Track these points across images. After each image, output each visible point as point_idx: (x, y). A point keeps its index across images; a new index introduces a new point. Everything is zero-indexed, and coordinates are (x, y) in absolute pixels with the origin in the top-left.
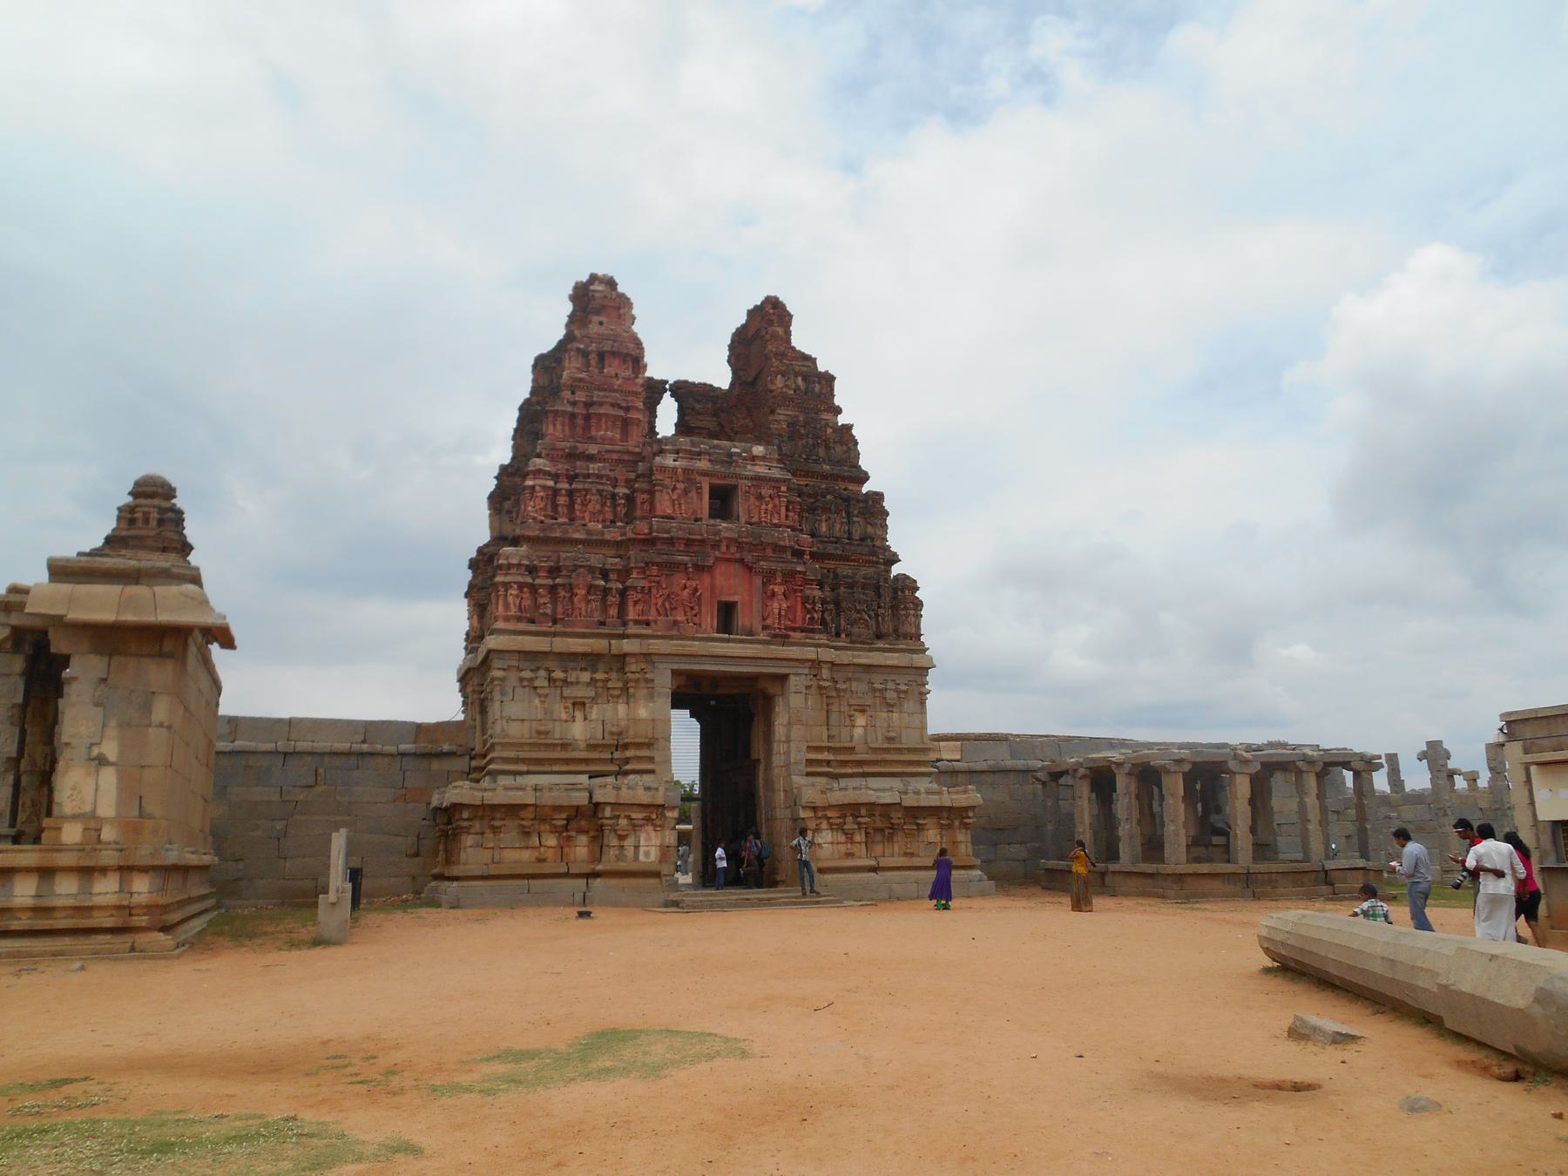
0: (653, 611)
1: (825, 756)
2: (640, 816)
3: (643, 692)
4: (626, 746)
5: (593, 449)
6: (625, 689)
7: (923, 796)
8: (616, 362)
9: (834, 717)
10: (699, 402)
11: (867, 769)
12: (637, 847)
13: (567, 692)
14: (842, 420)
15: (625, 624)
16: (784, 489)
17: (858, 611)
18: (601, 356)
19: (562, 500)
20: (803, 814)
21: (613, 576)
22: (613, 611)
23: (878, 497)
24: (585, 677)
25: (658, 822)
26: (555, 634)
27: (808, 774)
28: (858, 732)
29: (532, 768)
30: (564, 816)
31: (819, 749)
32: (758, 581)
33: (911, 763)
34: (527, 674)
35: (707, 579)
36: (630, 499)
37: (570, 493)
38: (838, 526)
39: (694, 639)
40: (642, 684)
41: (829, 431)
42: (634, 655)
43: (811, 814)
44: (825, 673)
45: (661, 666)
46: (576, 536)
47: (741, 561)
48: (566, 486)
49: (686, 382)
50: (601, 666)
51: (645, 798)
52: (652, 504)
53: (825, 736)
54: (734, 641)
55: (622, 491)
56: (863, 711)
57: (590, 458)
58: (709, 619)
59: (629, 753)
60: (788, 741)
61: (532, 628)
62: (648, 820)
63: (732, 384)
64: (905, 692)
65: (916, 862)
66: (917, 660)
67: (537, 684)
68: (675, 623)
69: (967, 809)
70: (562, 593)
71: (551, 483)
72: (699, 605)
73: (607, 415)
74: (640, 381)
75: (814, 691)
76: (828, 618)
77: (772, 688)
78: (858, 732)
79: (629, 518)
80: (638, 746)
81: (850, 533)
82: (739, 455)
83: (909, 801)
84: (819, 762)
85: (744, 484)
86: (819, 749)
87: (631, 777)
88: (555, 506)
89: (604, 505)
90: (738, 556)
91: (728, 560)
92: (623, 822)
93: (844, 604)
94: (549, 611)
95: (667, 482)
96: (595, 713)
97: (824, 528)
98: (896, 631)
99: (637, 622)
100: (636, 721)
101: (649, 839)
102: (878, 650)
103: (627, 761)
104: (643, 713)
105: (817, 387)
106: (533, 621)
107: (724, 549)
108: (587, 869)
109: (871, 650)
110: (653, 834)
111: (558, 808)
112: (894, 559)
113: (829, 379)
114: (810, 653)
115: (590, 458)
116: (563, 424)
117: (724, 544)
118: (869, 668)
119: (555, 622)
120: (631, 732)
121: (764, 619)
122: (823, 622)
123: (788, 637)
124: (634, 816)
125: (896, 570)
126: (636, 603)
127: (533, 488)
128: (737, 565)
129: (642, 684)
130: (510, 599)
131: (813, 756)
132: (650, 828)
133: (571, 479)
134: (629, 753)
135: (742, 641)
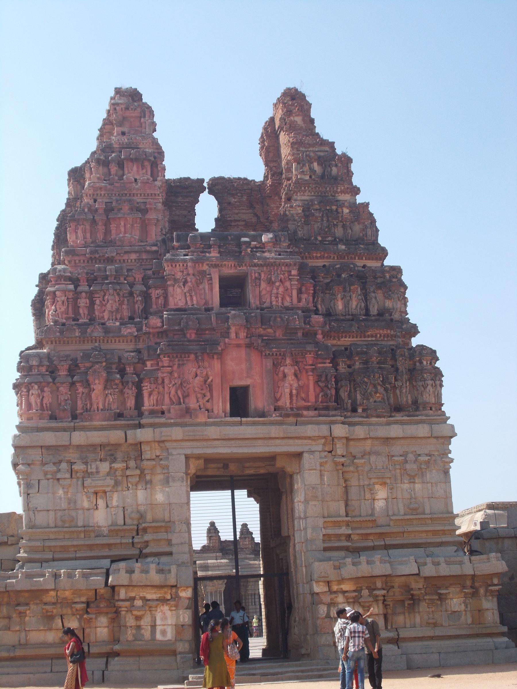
0: (167, 400)
1: (344, 530)
2: (155, 596)
3: (159, 477)
4: (145, 530)
5: (110, 252)
6: (142, 475)
7: (443, 565)
9: (354, 492)
10: (233, 195)
11: (389, 541)
12: (154, 627)
13: (88, 482)
14: (360, 199)
15: (141, 415)
16: (294, 272)
18: (121, 165)
19: (83, 302)
20: (318, 588)
21: (129, 369)
22: (131, 403)
23: (397, 271)
24: (104, 467)
25: (172, 603)
26: (74, 429)
27: (325, 549)
28: (380, 504)
29: (57, 556)
30: (84, 599)
31: (337, 524)
32: (269, 363)
33: (435, 533)
34: (51, 468)
36: (147, 297)
37: (91, 296)
38: (354, 304)
39: (206, 424)
40: (159, 470)
41: (346, 211)
42: (148, 442)
43: (326, 589)
44: (340, 450)
45: (174, 452)
46: (95, 334)
47: (249, 346)
48: (87, 288)
49: (222, 178)
50: (119, 455)
51: (154, 577)
52: (166, 298)
53: (343, 512)
54: (247, 424)
55: (139, 288)
56: (384, 484)
57: (110, 260)
58: (221, 404)
59: (147, 537)
61: (54, 424)
62: (163, 601)
63: (266, 177)
64: (428, 462)
65: (438, 632)
66: (438, 429)
67: (59, 476)
68: (188, 411)
69: (492, 576)
70: (81, 390)
71: (71, 287)
72: (211, 391)
74: (158, 183)
75: (329, 466)
76: (344, 394)
78: (380, 504)
79: (146, 313)
80: (156, 530)
81: (367, 309)
82: (248, 244)
83: (429, 571)
84: (338, 537)
85: (253, 272)
86: (337, 524)
87: (149, 559)
88: (76, 308)
89: (121, 303)
91: (238, 346)
92: (138, 603)
93: (358, 379)
94: (68, 407)
95: (179, 275)
96: (115, 500)
97: (340, 306)
98: (415, 402)
99: (152, 413)
100: (152, 505)
101: (164, 618)
102: (396, 422)
103: (147, 544)
104: (160, 497)
105: (334, 170)
106: (53, 417)
107: (233, 335)
108: (105, 649)
109: (388, 424)
110: (168, 613)
111: (77, 592)
112: (414, 330)
113: (347, 160)
114: (324, 430)
115: (110, 260)
116: (84, 232)
118: (387, 441)
119: (74, 417)
120: (149, 517)
121: (277, 400)
122: (338, 399)
123: (301, 416)
124: (149, 597)
125: (415, 342)
127: (54, 293)
129: (159, 470)
130: (32, 399)
131: (330, 531)
132: (166, 608)
133: (91, 282)
134: (147, 537)
135: (254, 424)
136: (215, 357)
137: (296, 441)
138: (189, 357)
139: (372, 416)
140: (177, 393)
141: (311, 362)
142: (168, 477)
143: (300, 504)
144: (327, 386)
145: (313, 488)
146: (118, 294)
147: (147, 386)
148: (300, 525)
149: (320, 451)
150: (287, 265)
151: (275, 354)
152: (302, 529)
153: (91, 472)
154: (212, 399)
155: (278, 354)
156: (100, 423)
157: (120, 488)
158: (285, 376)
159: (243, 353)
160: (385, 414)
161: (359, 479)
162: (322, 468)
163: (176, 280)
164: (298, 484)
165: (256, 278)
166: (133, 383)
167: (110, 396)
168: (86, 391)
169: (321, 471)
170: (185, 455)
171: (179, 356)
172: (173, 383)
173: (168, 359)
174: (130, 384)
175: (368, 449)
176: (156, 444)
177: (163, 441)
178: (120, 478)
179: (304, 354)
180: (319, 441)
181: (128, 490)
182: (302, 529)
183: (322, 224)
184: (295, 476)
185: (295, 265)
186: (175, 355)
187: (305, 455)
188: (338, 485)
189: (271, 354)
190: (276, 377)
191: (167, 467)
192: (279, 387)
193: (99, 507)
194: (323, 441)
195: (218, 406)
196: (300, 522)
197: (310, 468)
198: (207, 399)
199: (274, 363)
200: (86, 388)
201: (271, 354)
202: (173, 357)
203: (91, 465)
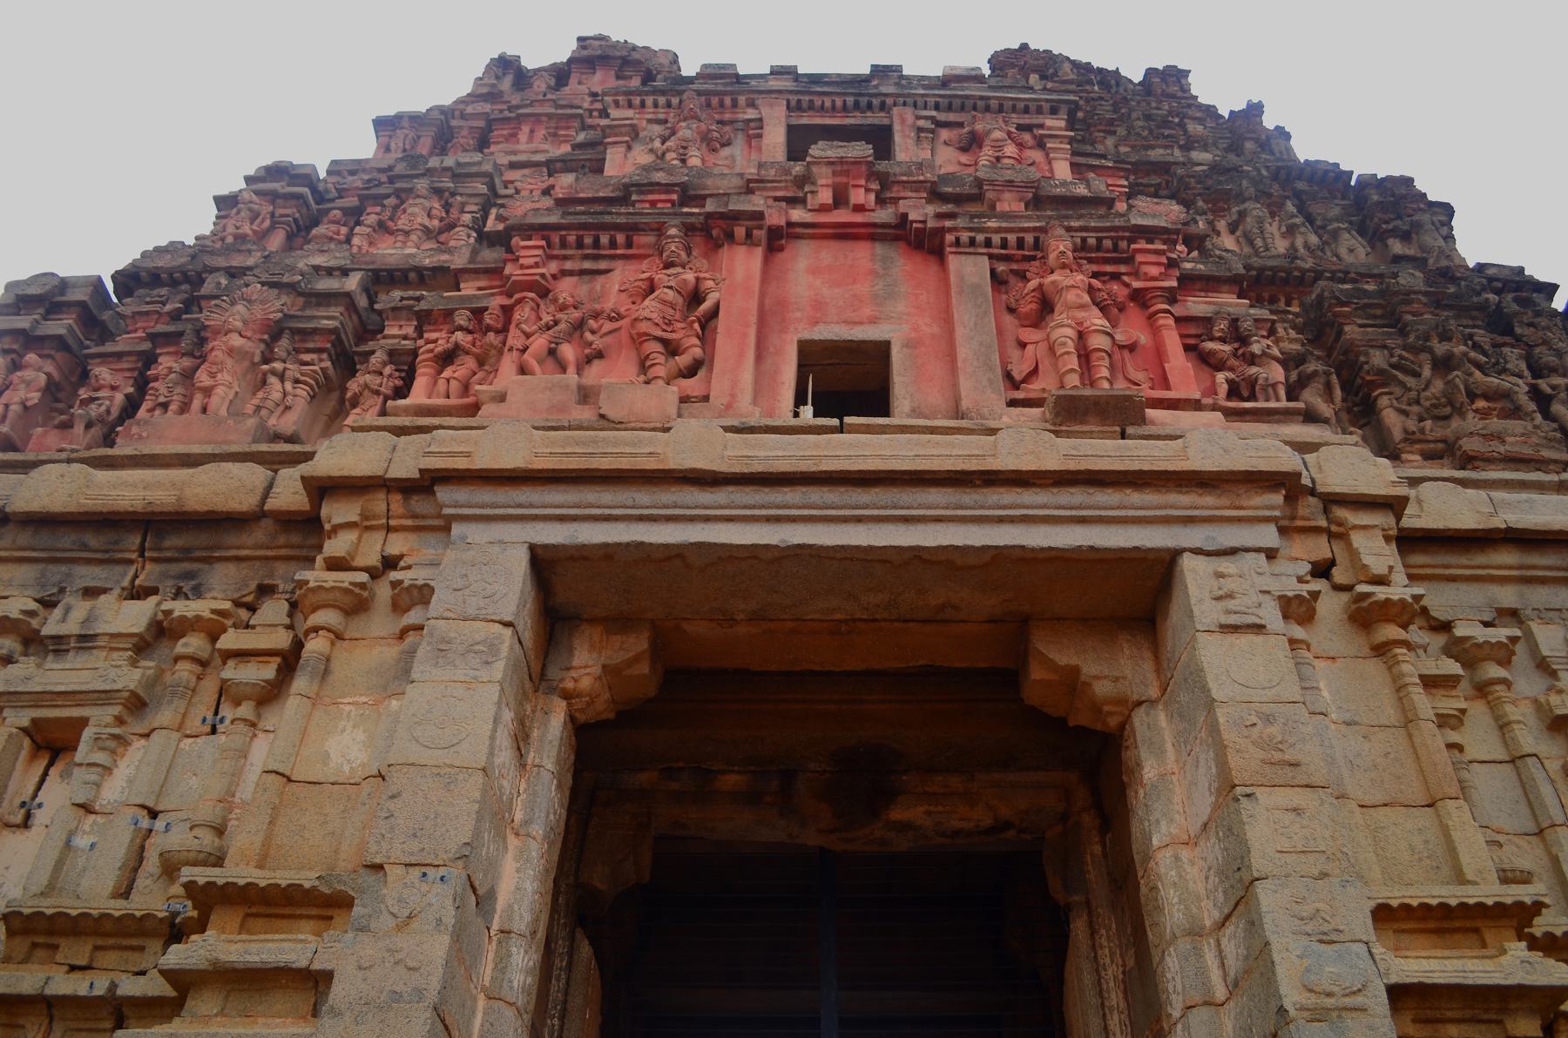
3: (369, 650)
8: (599, 75)
16: (1056, 123)
17: (1444, 365)
32: (970, 270)
35: (744, 263)
45: (477, 534)
60: (1241, 897)
70: (167, 363)
73: (537, 118)
77: (1111, 671)
90: (884, 215)
91: (844, 233)
96: (128, 777)
104: (345, 746)
117: (824, 177)
120: (244, 838)
126: (447, 358)
128: (879, 248)
129: (380, 623)
136: (740, 232)
137: (1135, 497)
138: (629, 245)
139: (1489, 461)
140: (552, 352)
141: (1154, 271)
142: (412, 652)
143: (1185, 854)
144: (1235, 355)
145: (1269, 719)
146: (447, 207)
147: (435, 341)
148: (1202, 972)
149: (1271, 554)
150: (1026, 110)
151: (996, 239)
152: (1220, 993)
153: (58, 639)
154: (711, 369)
155: (1012, 238)
156: (181, 449)
157: (165, 716)
158: (1046, 306)
159: (862, 254)
160: (1546, 453)
161: (1503, 726)
162: (1298, 632)
163: (634, 132)
164: (1160, 753)
165: (920, 130)
166: (393, 354)
167: (272, 380)
168: (187, 362)
169: (1292, 641)
170: (542, 562)
171: (588, 240)
172: (547, 318)
173: (543, 243)
174: (378, 358)
175: (1507, 596)
176: (396, 500)
177: (428, 482)
178: (185, 671)
179: (1123, 244)
180: (1259, 500)
181: (214, 731)
182: (1220, 993)
183: (1130, 129)
184: (1139, 719)
185: (1054, 112)
186: (572, 238)
187: (1188, 563)
188: (1408, 720)
189: (980, 238)
190: (1008, 319)
191: (423, 594)
192: (1023, 345)
193: (40, 817)
194: (1278, 498)
195: (735, 383)
196: (1199, 955)
197: (1233, 620)
198: (683, 360)
199: (993, 272)
200: (190, 354)
201: (980, 238)
202: (564, 245)
203: (68, 610)
